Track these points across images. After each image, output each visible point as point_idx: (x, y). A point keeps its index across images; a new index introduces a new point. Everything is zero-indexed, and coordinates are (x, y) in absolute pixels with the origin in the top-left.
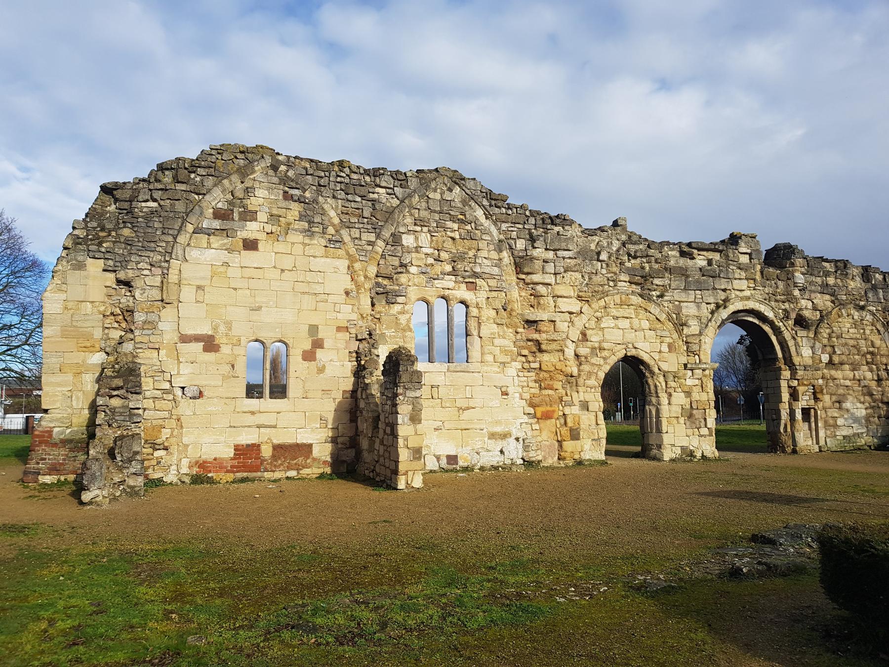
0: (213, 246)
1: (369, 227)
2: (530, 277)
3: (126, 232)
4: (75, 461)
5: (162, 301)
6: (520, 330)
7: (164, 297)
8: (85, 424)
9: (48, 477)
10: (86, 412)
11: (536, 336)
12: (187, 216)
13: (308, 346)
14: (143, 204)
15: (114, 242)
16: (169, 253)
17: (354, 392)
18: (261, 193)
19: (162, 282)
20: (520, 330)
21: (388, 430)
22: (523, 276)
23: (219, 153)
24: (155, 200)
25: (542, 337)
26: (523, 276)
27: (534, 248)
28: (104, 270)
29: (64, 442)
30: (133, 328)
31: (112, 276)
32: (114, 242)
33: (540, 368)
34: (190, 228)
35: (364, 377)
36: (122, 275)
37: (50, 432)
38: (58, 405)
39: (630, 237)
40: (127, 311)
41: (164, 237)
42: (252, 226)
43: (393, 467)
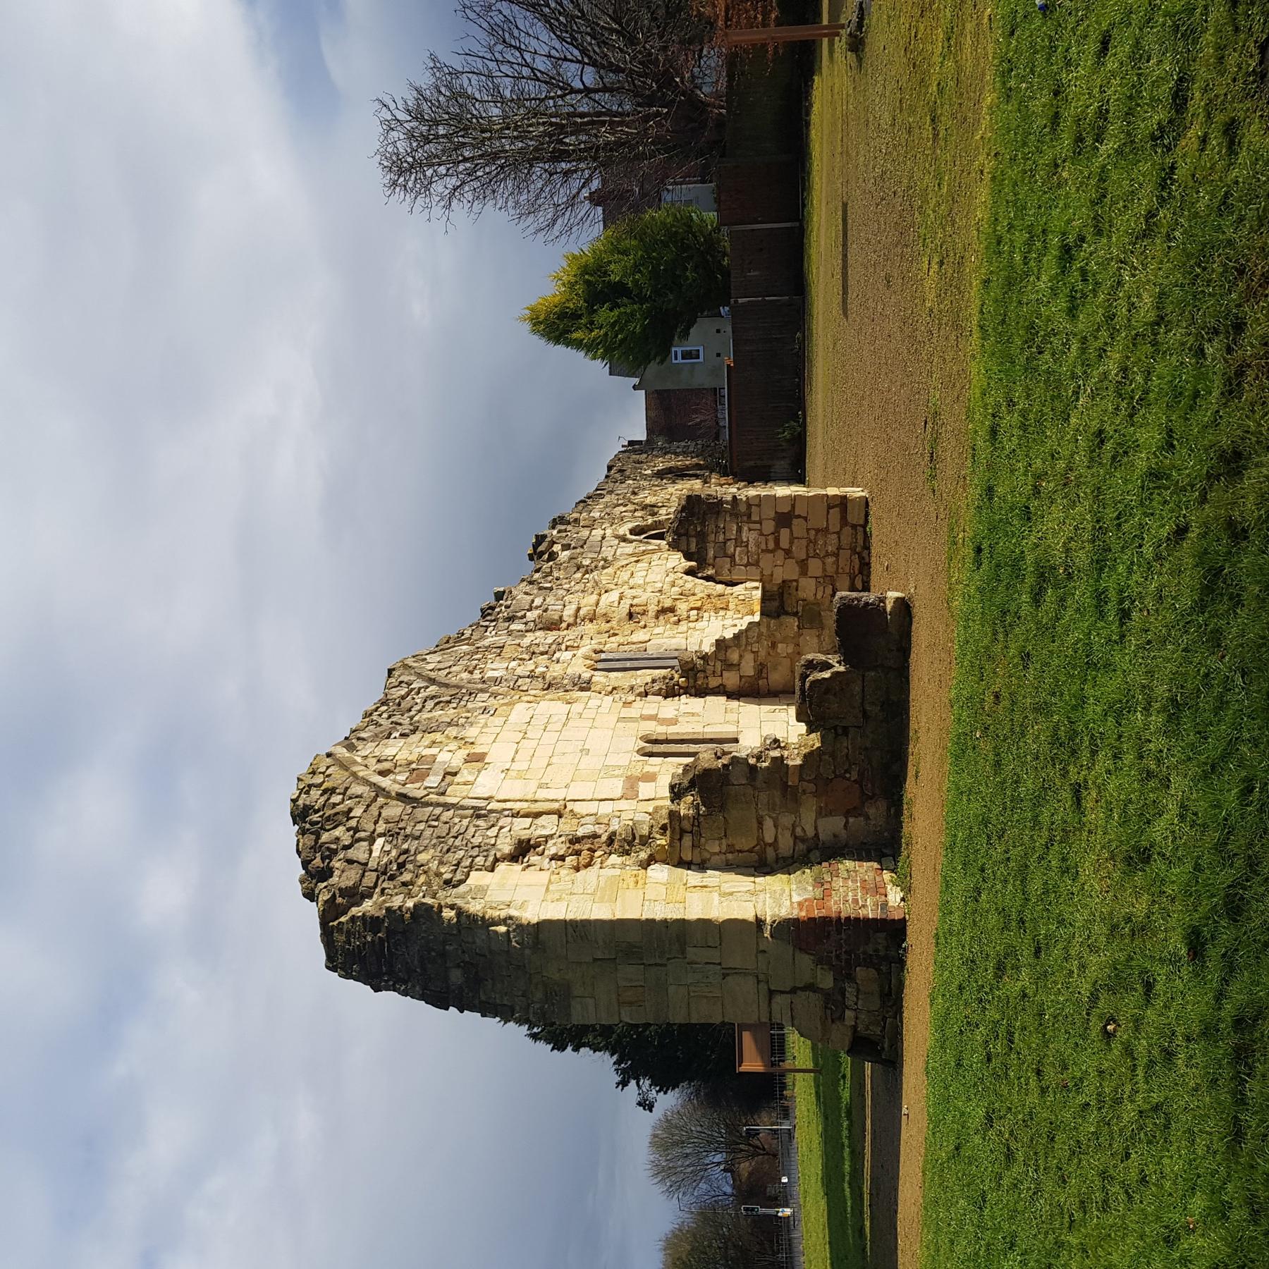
0: (471, 778)
1: (466, 698)
2: (565, 618)
3: (422, 858)
4: (855, 871)
5: (560, 817)
6: (642, 623)
7: (556, 806)
8: (785, 877)
9: (890, 897)
10: (758, 880)
11: (651, 614)
12: (415, 800)
13: (654, 723)
14: (376, 854)
15: (441, 863)
16: (477, 813)
17: (731, 695)
18: (389, 752)
19: (526, 816)
20: (642, 623)
21: (785, 533)
22: (564, 625)
23: (308, 793)
24: (371, 840)
25: (653, 608)
26: (564, 625)
27: (524, 616)
28: (492, 871)
29: (819, 882)
30: (604, 838)
31: (502, 867)
32: (441, 863)
33: (698, 609)
34: (433, 798)
35: (705, 657)
36: (506, 847)
37: (800, 904)
38: (751, 904)
39: (523, 580)
40: (571, 842)
41: (443, 818)
42: (443, 757)
43: (835, 513)
